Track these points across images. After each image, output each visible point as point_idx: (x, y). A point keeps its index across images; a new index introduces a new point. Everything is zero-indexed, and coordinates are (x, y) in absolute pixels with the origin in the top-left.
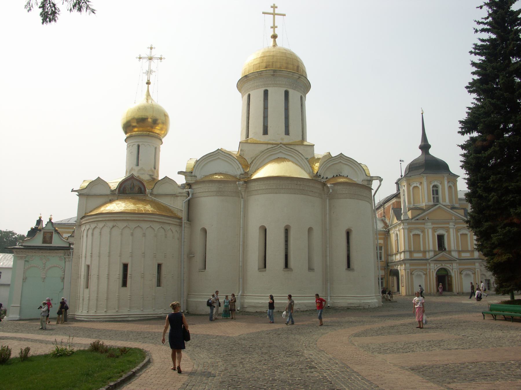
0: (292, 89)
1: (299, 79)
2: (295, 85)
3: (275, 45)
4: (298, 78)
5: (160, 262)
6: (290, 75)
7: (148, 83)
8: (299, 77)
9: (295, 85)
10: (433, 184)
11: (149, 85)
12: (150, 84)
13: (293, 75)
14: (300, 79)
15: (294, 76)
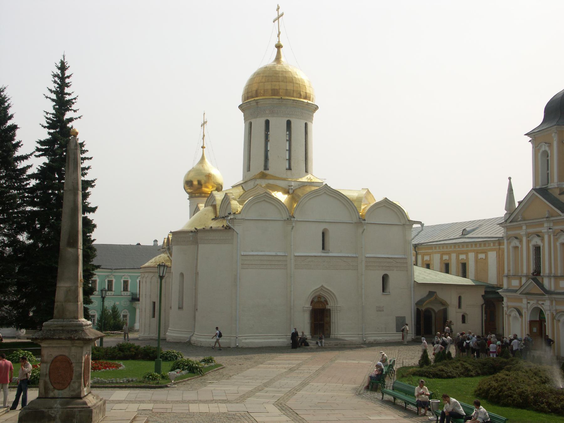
0: (254, 118)
1: (257, 104)
2: (256, 112)
3: (278, 58)
4: (255, 104)
5: (154, 301)
6: (248, 105)
7: (203, 147)
8: (257, 103)
9: (256, 112)
10: (541, 151)
11: (204, 149)
12: (205, 148)
13: (250, 104)
14: (258, 103)
15: (252, 104)
